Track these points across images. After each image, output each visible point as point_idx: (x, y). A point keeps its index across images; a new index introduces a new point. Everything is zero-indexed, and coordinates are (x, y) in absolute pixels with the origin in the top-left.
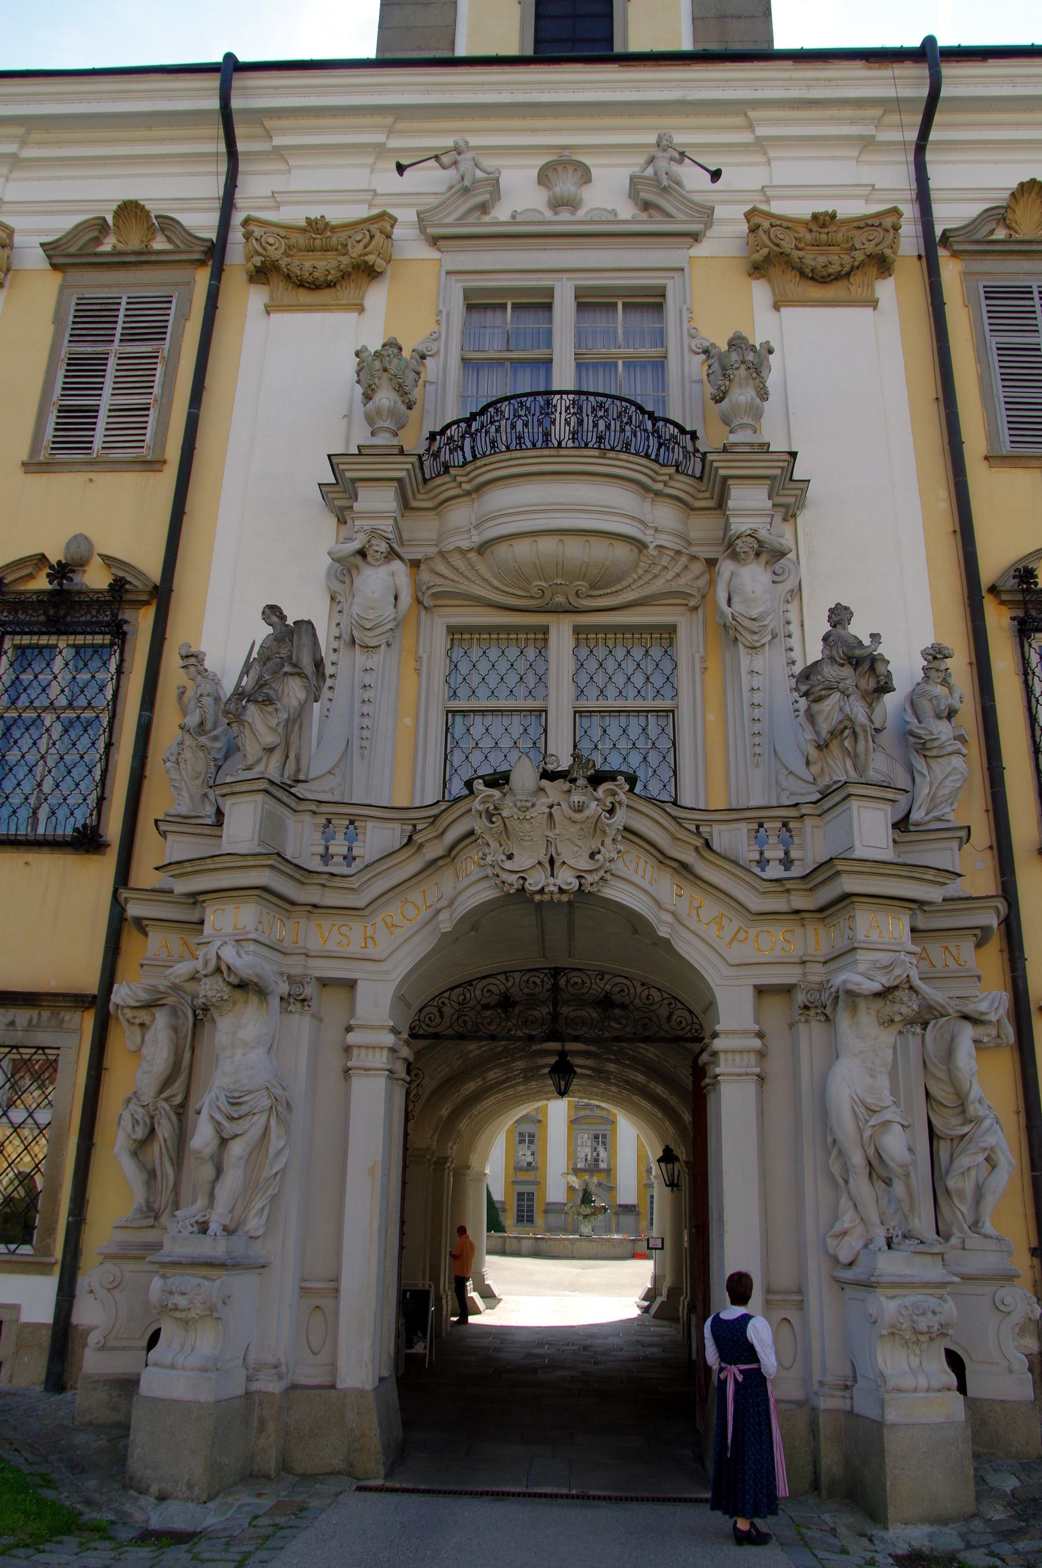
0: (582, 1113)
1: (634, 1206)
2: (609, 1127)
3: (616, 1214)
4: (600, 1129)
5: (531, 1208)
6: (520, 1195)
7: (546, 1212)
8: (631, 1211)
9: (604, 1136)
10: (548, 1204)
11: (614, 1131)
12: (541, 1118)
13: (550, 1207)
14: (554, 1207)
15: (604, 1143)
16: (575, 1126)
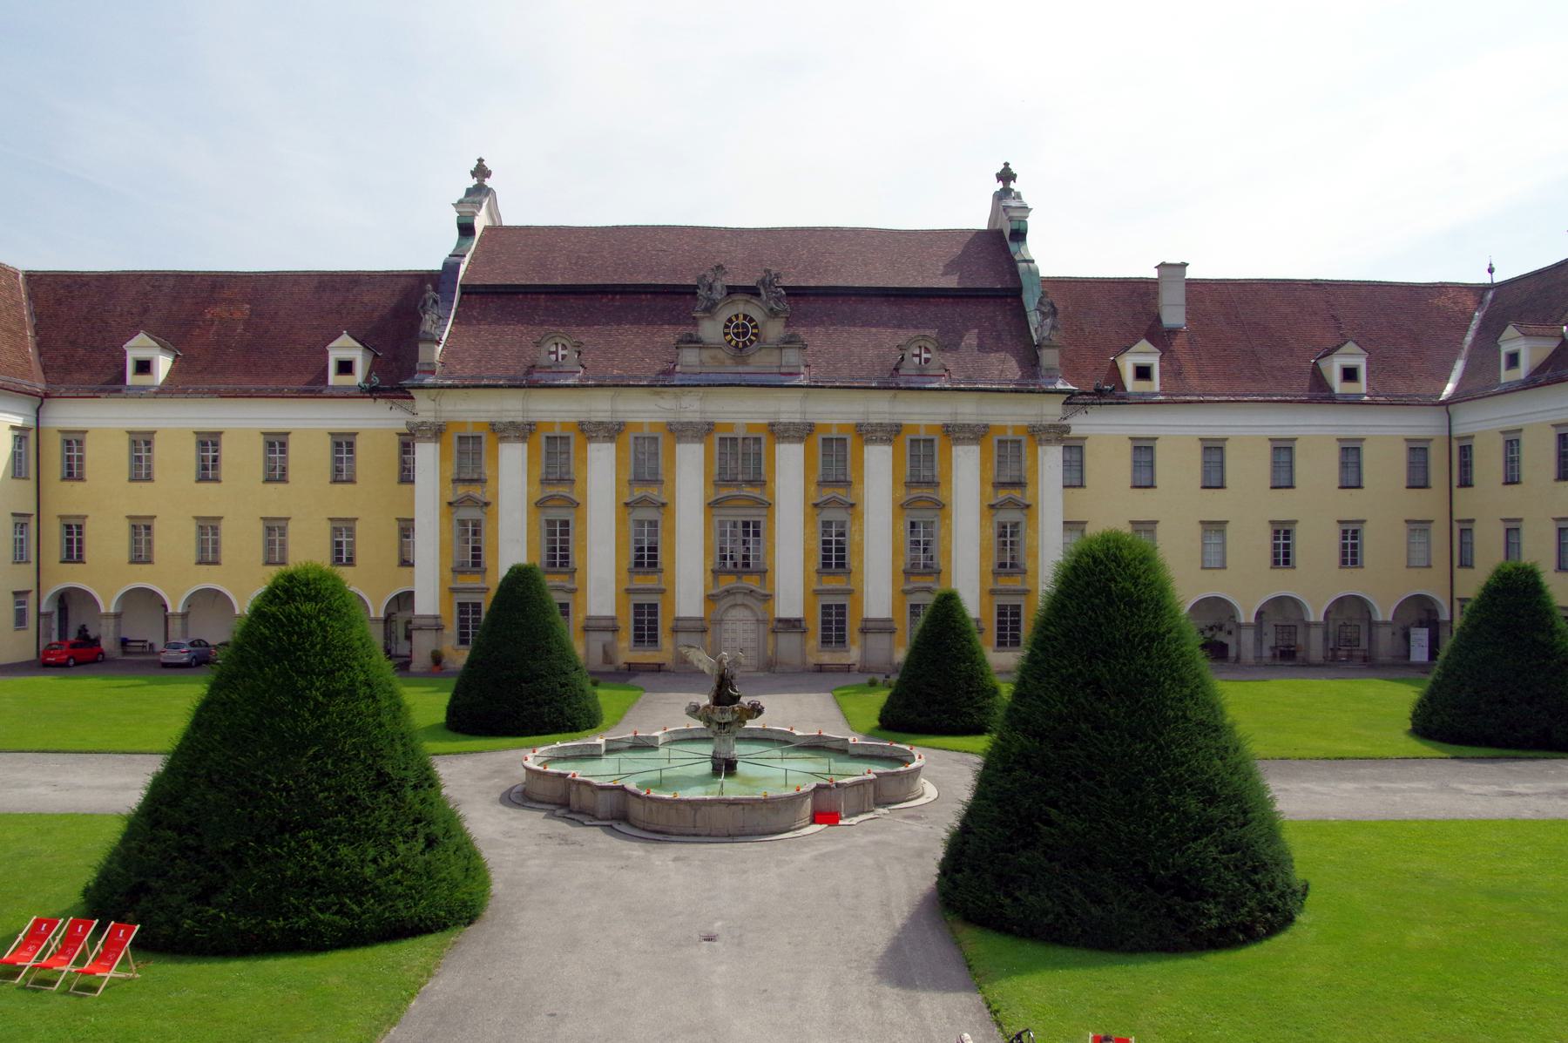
0: (725, 492)
1: (799, 620)
2: (764, 512)
3: (774, 631)
4: (751, 515)
5: (653, 627)
6: (638, 608)
7: (675, 631)
8: (794, 627)
9: (757, 524)
10: (678, 619)
11: (771, 518)
12: (665, 501)
13: (680, 623)
14: (687, 624)
15: (757, 534)
16: (715, 511)
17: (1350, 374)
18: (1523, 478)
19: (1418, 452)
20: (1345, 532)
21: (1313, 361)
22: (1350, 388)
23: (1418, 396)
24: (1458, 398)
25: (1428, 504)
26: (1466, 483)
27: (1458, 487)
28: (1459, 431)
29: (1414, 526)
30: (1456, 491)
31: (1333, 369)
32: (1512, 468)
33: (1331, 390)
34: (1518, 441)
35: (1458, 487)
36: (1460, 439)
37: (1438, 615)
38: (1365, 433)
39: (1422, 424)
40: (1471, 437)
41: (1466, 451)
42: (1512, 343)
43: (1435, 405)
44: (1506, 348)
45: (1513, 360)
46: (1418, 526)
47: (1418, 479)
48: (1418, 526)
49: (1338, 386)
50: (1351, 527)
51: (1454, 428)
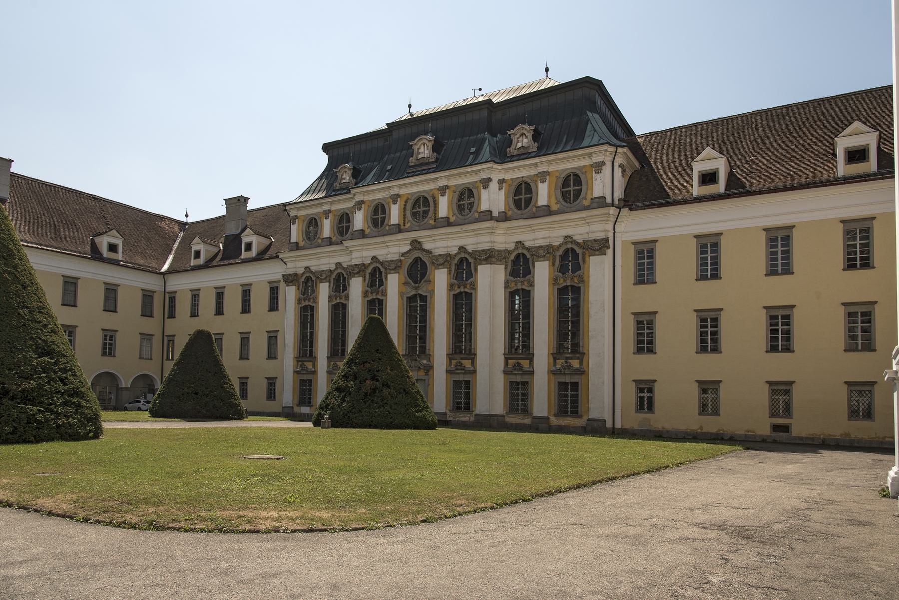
17: (112, 248)
18: (200, 314)
19: (148, 297)
20: (106, 336)
21: (91, 238)
22: (112, 255)
23: (149, 267)
24: (169, 272)
25: (151, 326)
26: (172, 316)
27: (167, 318)
28: (168, 289)
29: (143, 337)
30: (166, 319)
31: (103, 242)
32: (195, 309)
33: (101, 255)
34: (198, 295)
35: (167, 318)
36: (169, 293)
37: (154, 386)
38: (119, 282)
39: (151, 283)
40: (175, 292)
41: (172, 300)
42: (197, 245)
43: (157, 273)
44: (194, 248)
45: (197, 254)
46: (146, 337)
47: (147, 311)
48: (146, 337)
49: (105, 253)
50: (109, 334)
51: (166, 287)
